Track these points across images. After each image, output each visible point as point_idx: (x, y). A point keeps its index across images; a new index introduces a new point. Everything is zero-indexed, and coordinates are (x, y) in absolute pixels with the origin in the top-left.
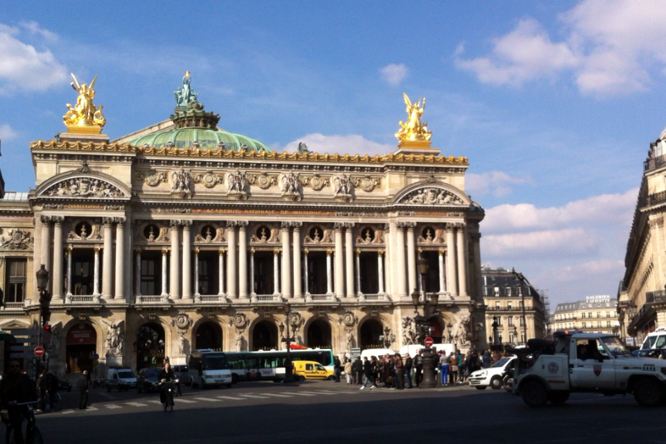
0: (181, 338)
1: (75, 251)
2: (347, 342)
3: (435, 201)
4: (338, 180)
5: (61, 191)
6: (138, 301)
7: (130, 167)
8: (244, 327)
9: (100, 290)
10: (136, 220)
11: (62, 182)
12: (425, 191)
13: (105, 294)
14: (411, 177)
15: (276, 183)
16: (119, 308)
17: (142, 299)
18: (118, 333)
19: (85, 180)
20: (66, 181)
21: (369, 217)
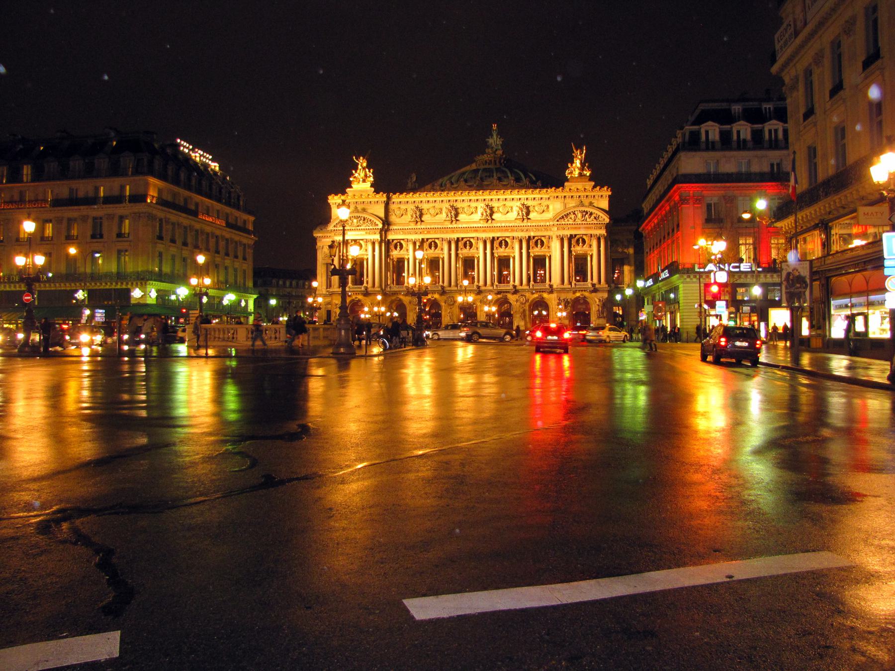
6: (388, 289)
15: (476, 212)
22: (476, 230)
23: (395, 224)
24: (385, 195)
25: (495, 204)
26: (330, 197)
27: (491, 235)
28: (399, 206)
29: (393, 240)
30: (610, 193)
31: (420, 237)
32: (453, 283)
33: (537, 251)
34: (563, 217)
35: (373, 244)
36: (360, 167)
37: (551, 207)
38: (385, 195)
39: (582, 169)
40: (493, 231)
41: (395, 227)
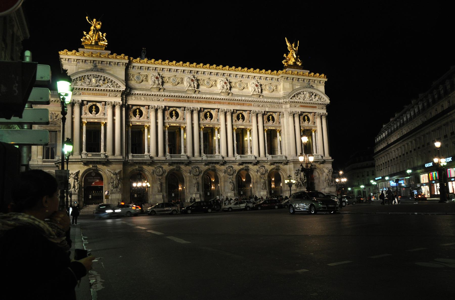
0: (159, 182)
1: (88, 124)
2: (262, 185)
3: (311, 99)
4: (253, 85)
5: (79, 83)
6: (130, 157)
7: (124, 70)
8: (198, 175)
9: (105, 150)
10: (128, 105)
11: (80, 77)
12: (305, 93)
13: (109, 152)
14: (295, 85)
16: (117, 162)
17: (133, 156)
18: (118, 178)
19: (95, 76)
20: (82, 76)
21: (272, 107)
22: (220, 101)
23: (136, 89)
24: (126, 57)
25: (233, 79)
26: (61, 53)
27: (232, 108)
28: (139, 71)
29: (133, 105)
30: (326, 80)
31: (163, 104)
32: (196, 154)
33: (271, 125)
34: (294, 96)
35: (114, 107)
36: (92, 28)
37: (281, 87)
38: (126, 57)
39: (296, 59)
40: (234, 104)
41: (137, 92)
